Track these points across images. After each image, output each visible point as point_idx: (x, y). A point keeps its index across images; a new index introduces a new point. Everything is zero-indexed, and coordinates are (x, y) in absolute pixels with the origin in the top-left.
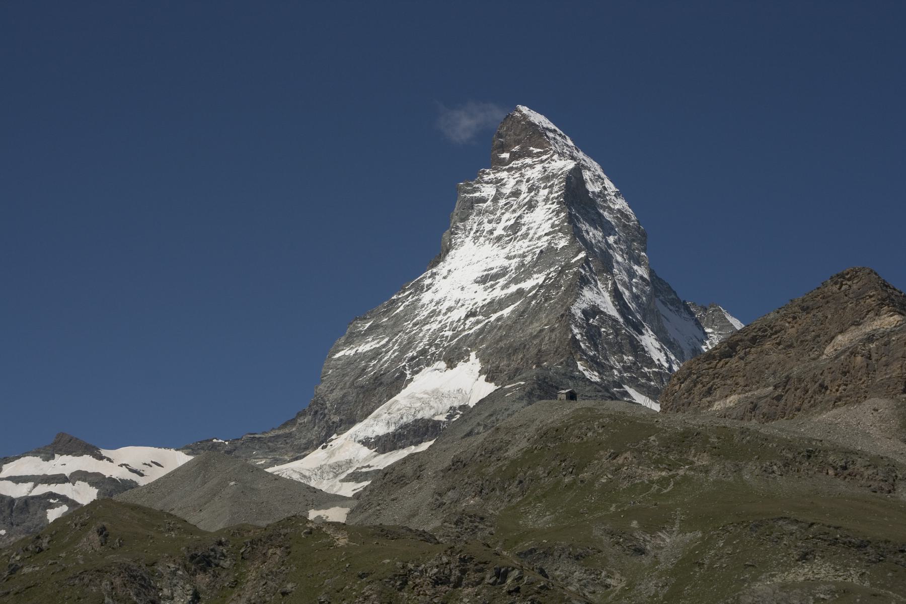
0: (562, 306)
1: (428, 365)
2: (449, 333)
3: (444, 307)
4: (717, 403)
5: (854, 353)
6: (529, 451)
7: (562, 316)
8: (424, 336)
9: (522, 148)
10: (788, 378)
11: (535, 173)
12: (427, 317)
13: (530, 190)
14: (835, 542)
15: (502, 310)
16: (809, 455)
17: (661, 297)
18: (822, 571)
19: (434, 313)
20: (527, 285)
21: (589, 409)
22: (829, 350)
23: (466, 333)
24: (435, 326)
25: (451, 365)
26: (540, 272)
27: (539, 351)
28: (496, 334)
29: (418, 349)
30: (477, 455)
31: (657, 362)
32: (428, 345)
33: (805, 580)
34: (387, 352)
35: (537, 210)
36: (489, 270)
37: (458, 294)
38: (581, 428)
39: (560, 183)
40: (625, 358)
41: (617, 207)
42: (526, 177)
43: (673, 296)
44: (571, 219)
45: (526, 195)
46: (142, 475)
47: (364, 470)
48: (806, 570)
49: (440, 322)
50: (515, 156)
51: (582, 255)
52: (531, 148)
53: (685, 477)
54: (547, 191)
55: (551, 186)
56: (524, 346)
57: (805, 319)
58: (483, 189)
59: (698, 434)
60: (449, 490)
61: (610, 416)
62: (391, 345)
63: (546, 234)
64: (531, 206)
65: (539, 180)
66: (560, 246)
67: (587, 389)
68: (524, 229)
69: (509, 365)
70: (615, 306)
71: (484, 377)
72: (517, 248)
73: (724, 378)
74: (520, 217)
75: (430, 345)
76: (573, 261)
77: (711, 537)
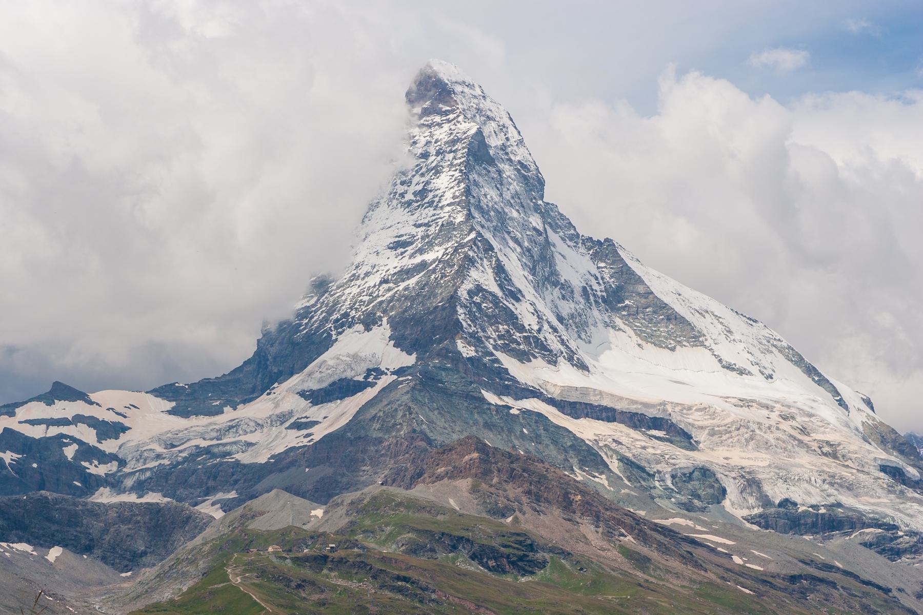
1: (350, 327)
2: (366, 298)
8: (346, 300)
11: (442, 134)
12: (347, 282)
13: (438, 153)
15: (408, 279)
17: (561, 234)
18: (410, 535)
19: (355, 277)
20: (429, 257)
23: (380, 299)
24: (355, 290)
25: (368, 329)
26: (440, 245)
27: (433, 326)
31: (527, 327)
34: (316, 312)
35: (443, 175)
36: (399, 237)
37: (373, 259)
39: (464, 148)
40: (501, 327)
41: (518, 158)
42: (435, 137)
45: (434, 157)
46: (125, 417)
47: (303, 420)
51: (473, 235)
52: (441, 106)
54: (452, 155)
55: (455, 151)
63: (448, 205)
64: (437, 170)
65: (446, 143)
66: (457, 221)
68: (431, 195)
70: (496, 281)
71: (392, 342)
72: (424, 216)
74: (428, 183)
75: (351, 308)
76: (465, 241)
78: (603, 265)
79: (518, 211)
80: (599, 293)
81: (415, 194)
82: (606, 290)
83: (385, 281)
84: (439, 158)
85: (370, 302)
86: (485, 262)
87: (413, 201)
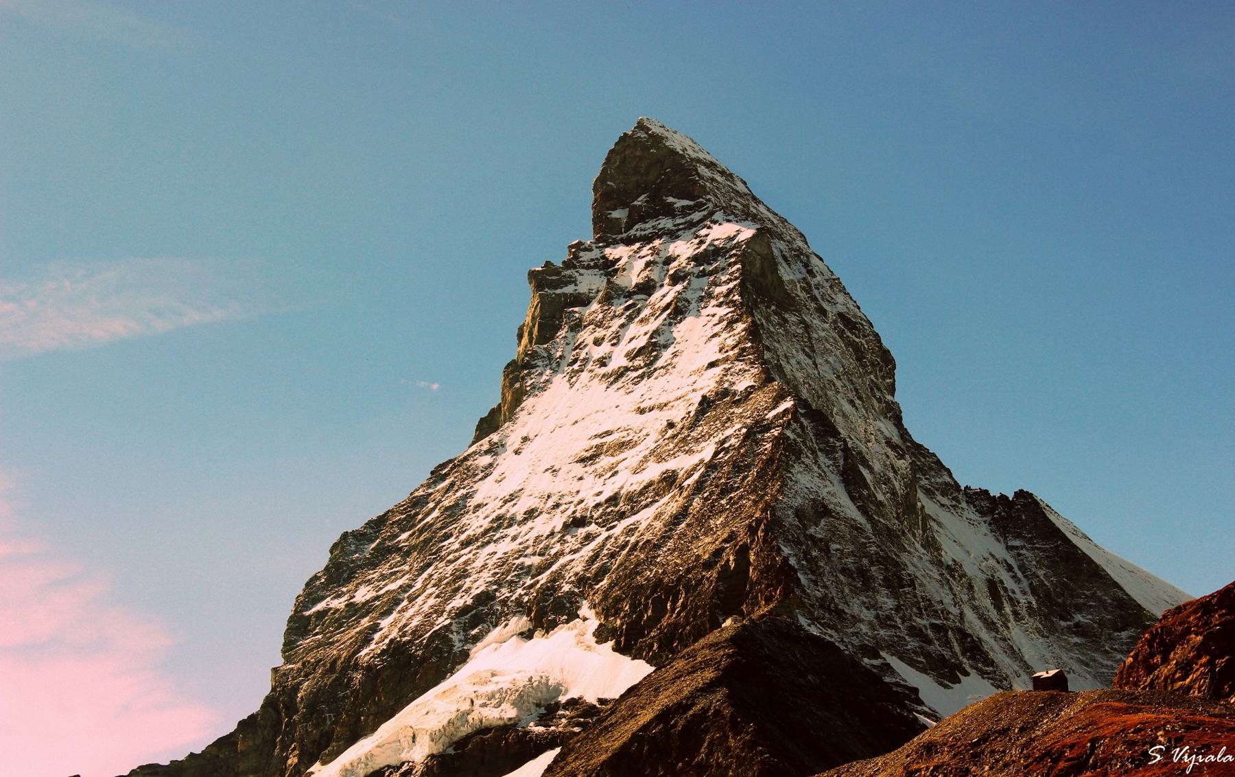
0: (755, 503)
3: (519, 510)
9: (655, 198)
19: (501, 522)
29: (475, 592)
32: (495, 583)
37: (546, 484)
42: (664, 255)
43: (947, 479)
44: (754, 332)
49: (514, 538)
50: (638, 216)
52: (670, 199)
55: (715, 271)
58: (579, 278)
62: (418, 585)
68: (666, 355)
74: (656, 332)
78: (1017, 543)
79: (852, 402)
80: (1019, 596)
81: (632, 356)
82: (1034, 591)
83: (579, 522)
84: (679, 287)
85: (541, 569)
86: (822, 458)
87: (627, 369)
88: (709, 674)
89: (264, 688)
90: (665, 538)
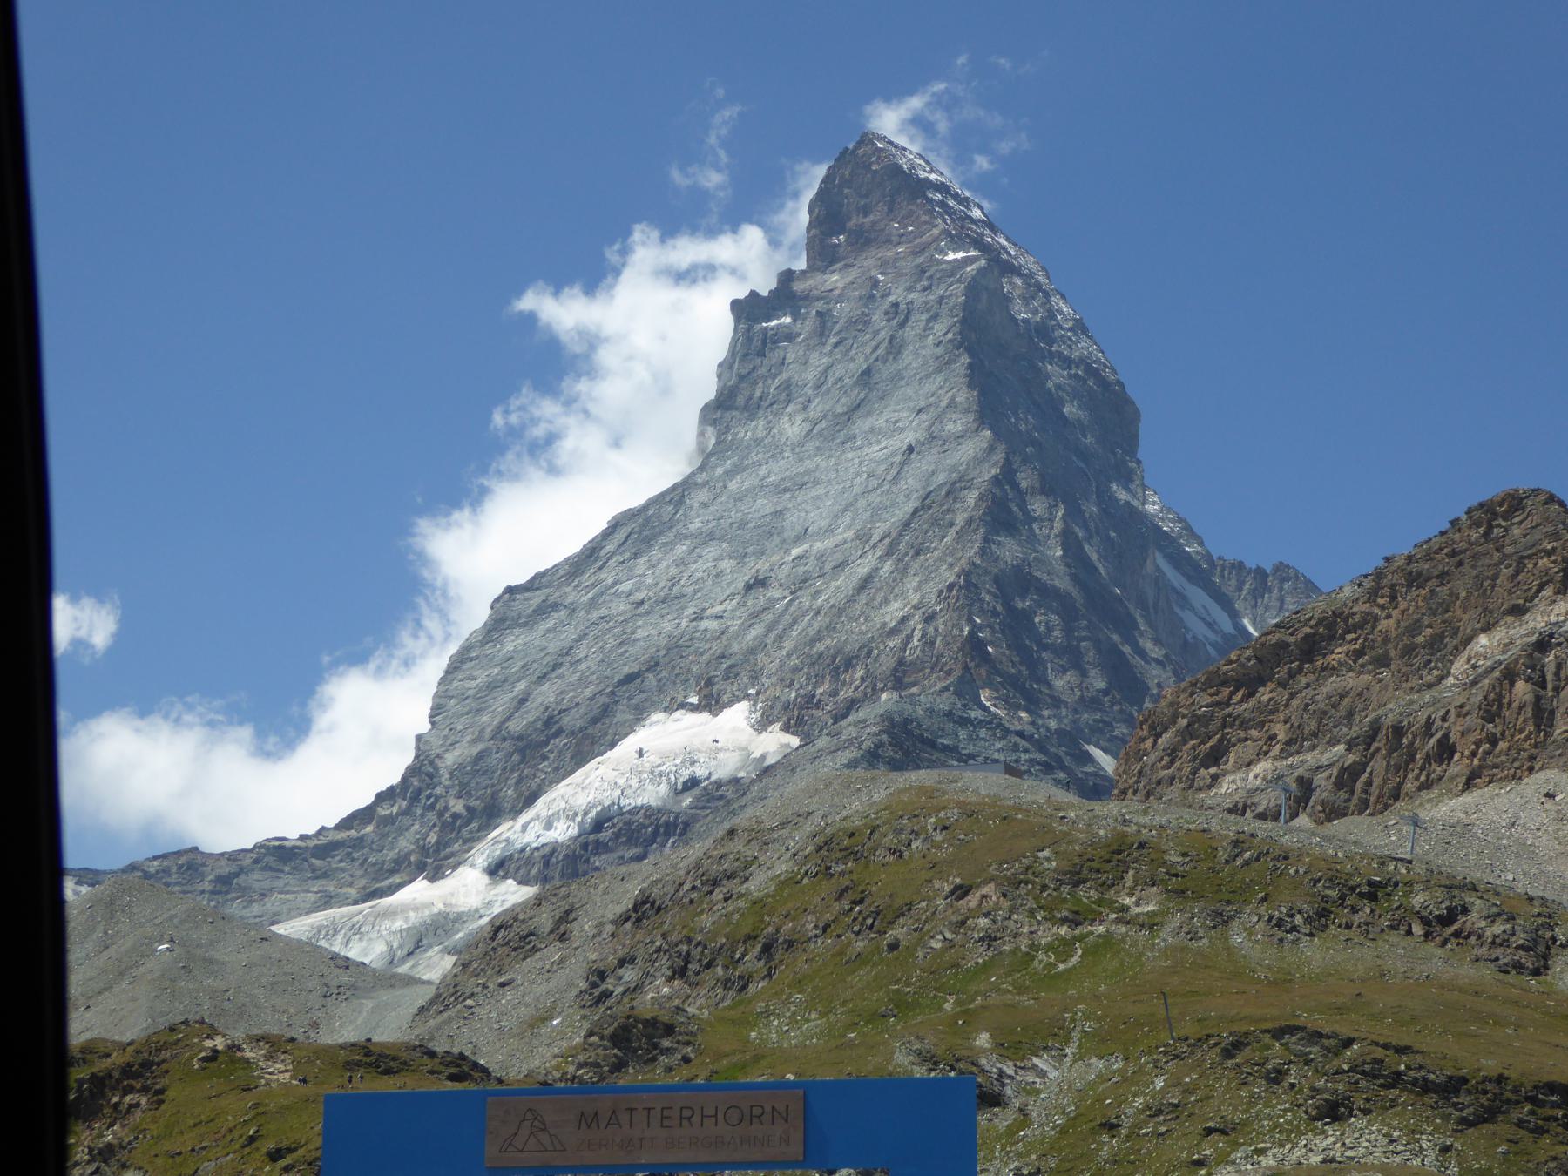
4: (1228, 778)
5: (1510, 676)
6: (793, 881)
7: (951, 587)
10: (1375, 728)
14: (1396, 1079)
16: (1373, 892)
21: (922, 790)
22: (1459, 666)
27: (901, 662)
28: (810, 625)
30: (686, 887)
33: (1324, 1161)
38: (898, 832)
48: (1332, 1139)
53: (1107, 936)
56: (866, 650)
57: (1414, 600)
59: (1142, 846)
60: (622, 963)
61: (959, 804)
67: (998, 745)
69: (835, 693)
73: (1245, 725)
77: (1140, 1070)
88: (848, 755)
89: (408, 758)
90: (851, 600)
